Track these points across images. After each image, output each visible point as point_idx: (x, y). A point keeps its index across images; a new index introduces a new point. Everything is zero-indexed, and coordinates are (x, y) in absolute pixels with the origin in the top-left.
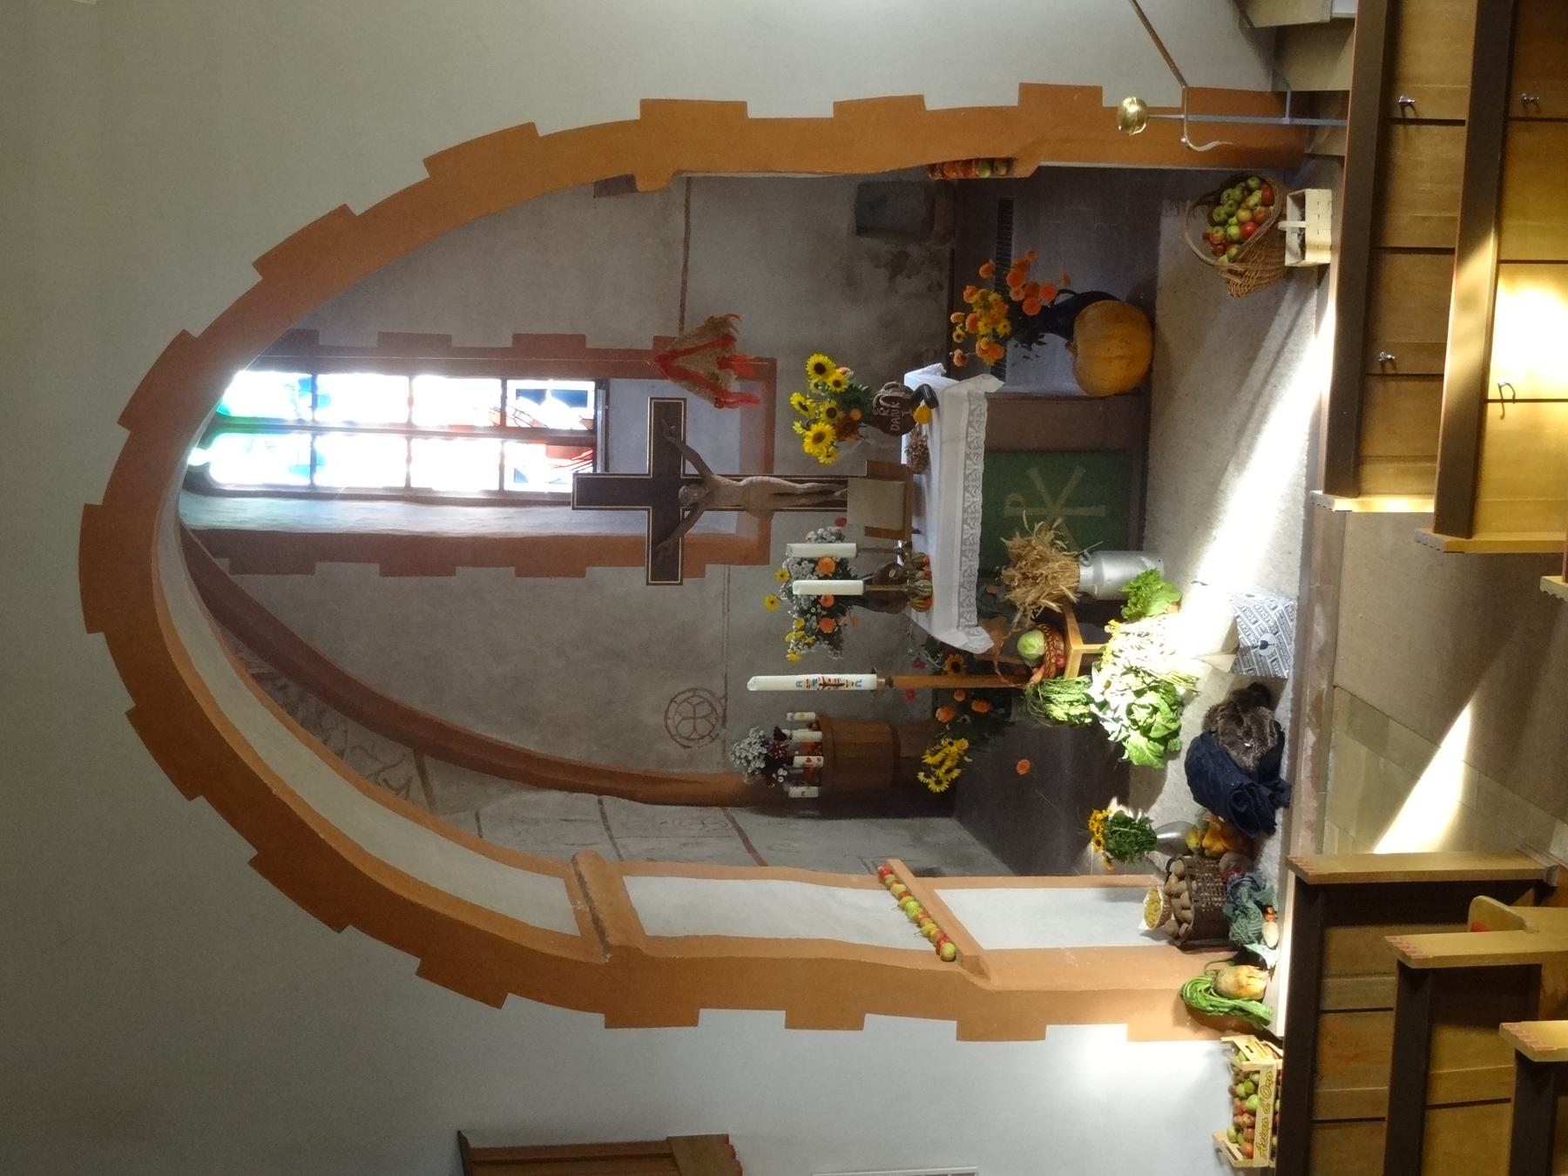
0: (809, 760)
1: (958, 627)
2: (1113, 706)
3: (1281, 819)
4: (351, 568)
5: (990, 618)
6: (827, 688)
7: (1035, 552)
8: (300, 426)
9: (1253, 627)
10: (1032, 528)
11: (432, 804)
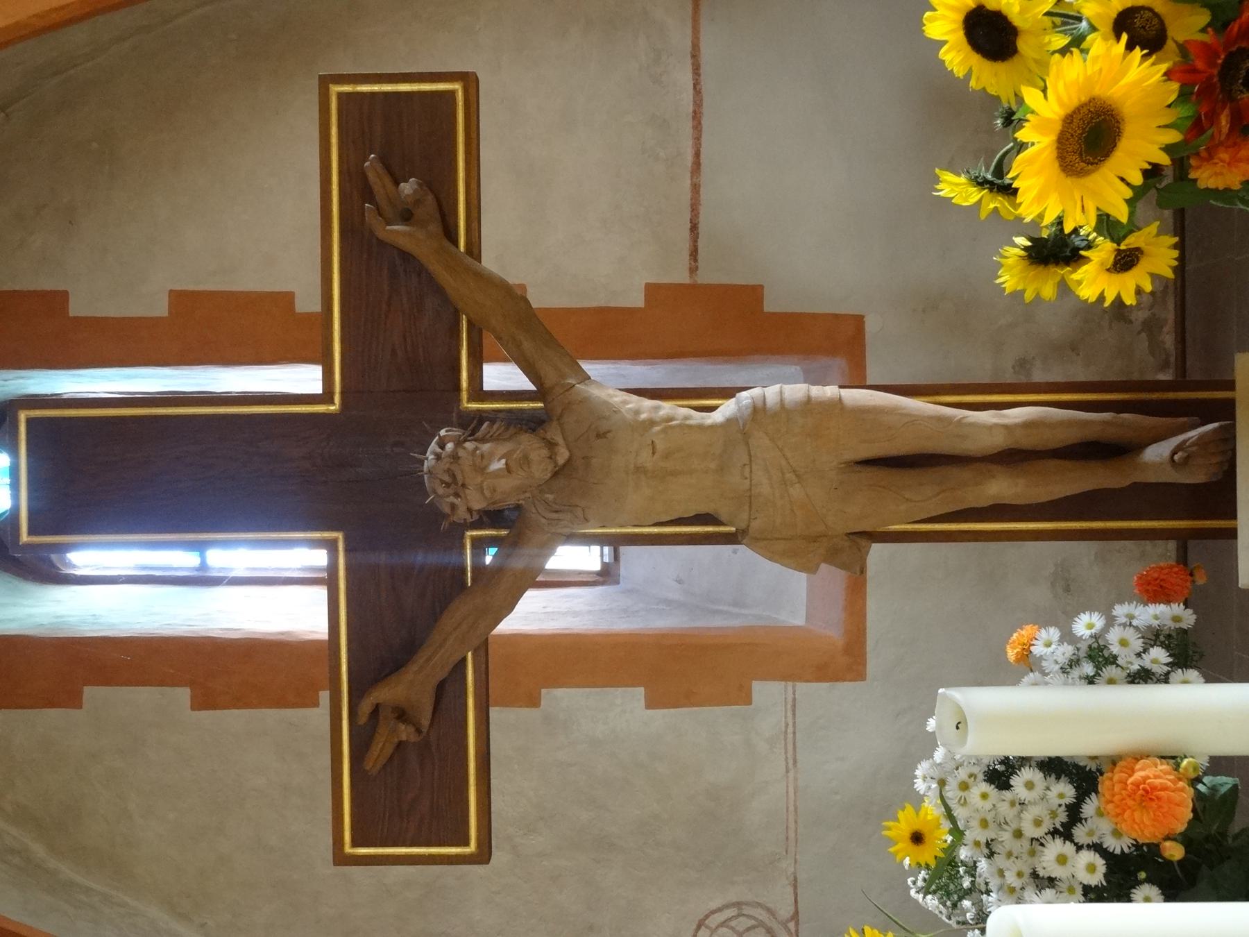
4: (144, 695)
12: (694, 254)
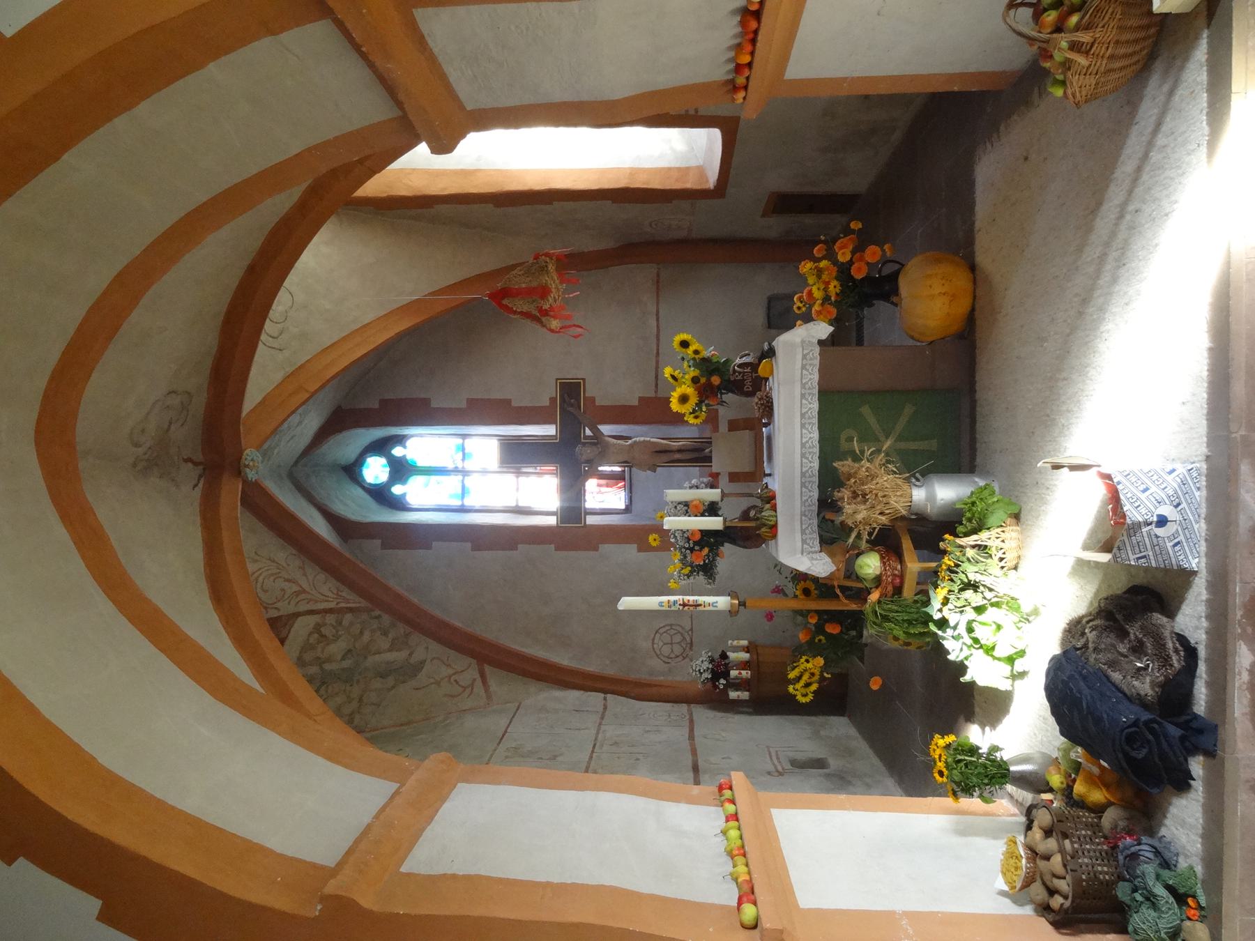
0: (740, 673)
1: (802, 554)
2: (952, 623)
3: (1201, 772)
5: (832, 543)
6: (686, 608)
7: (864, 469)
8: (456, 471)
9: (1143, 496)
10: (862, 452)
11: (489, 697)
12: (657, 385)
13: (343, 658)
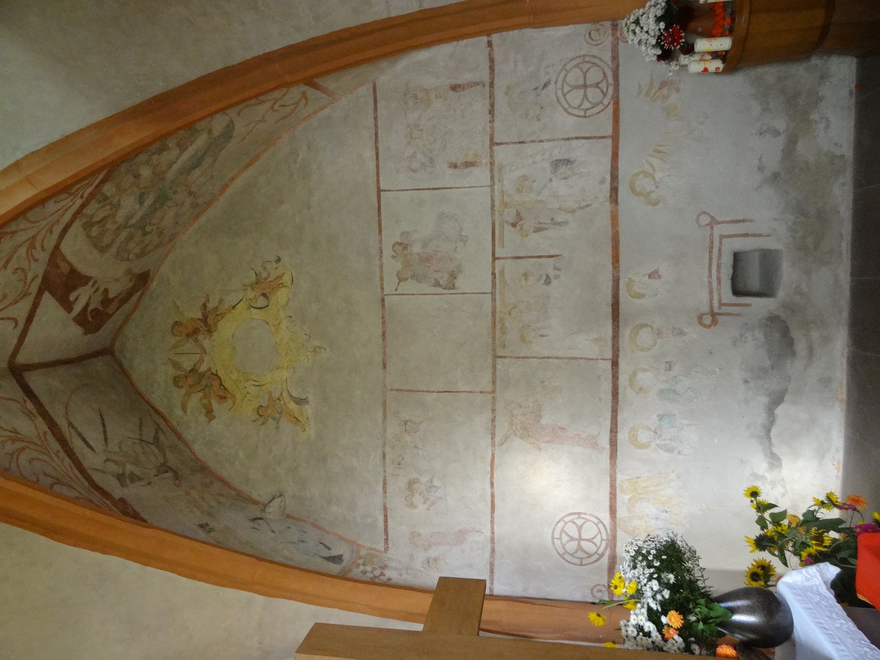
13: (141, 203)
